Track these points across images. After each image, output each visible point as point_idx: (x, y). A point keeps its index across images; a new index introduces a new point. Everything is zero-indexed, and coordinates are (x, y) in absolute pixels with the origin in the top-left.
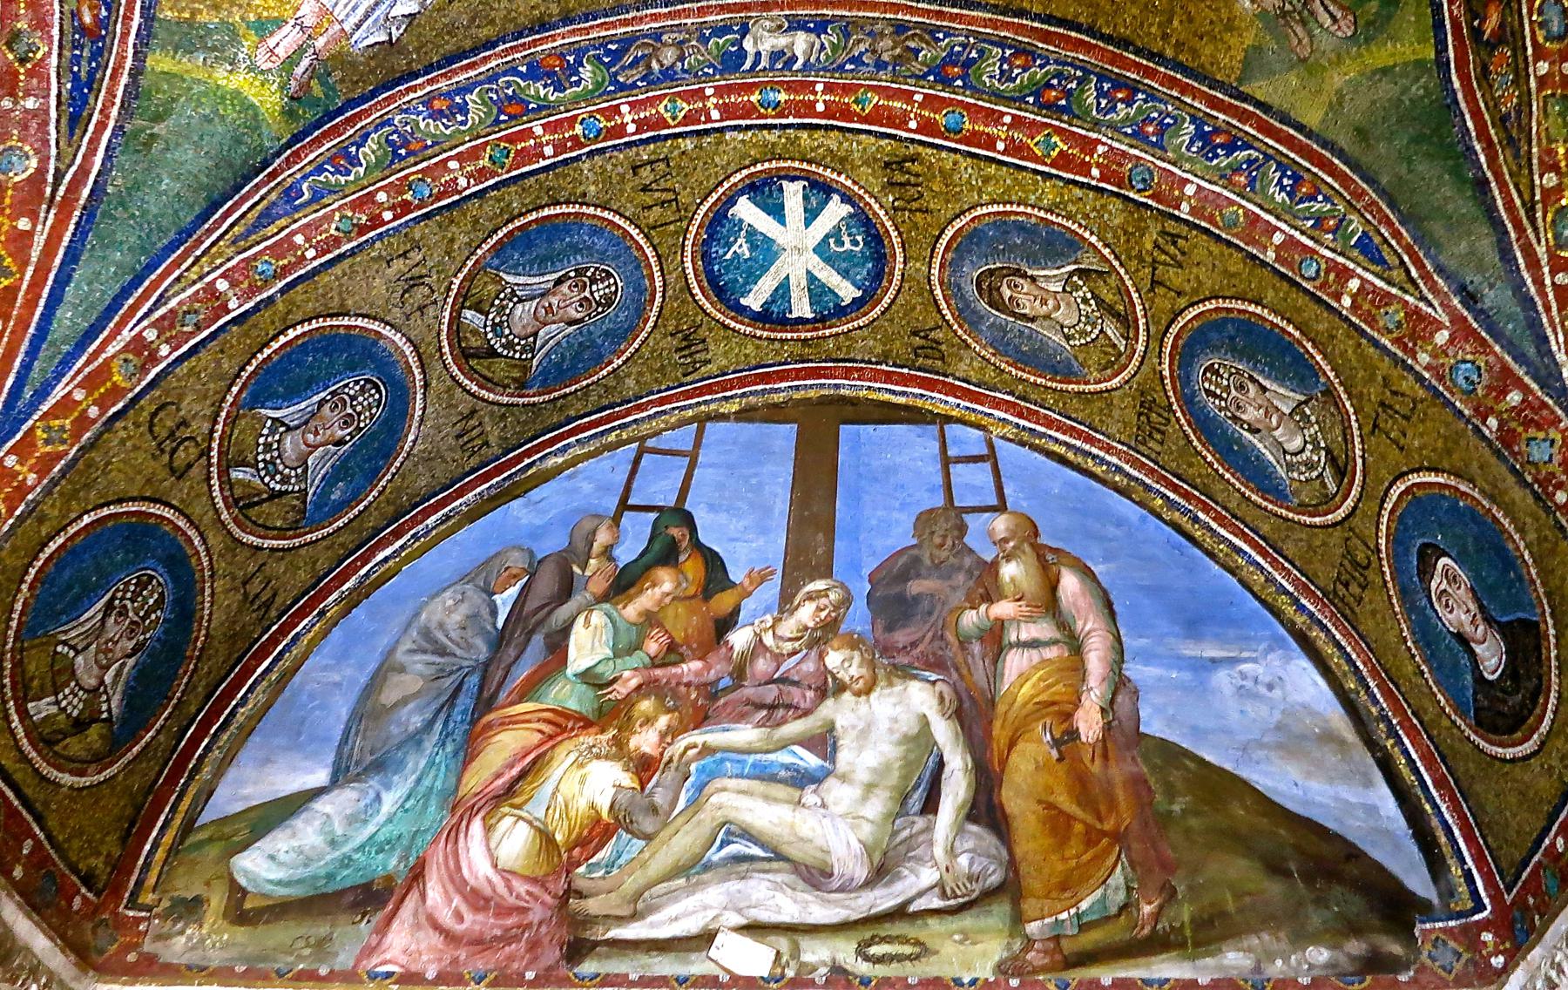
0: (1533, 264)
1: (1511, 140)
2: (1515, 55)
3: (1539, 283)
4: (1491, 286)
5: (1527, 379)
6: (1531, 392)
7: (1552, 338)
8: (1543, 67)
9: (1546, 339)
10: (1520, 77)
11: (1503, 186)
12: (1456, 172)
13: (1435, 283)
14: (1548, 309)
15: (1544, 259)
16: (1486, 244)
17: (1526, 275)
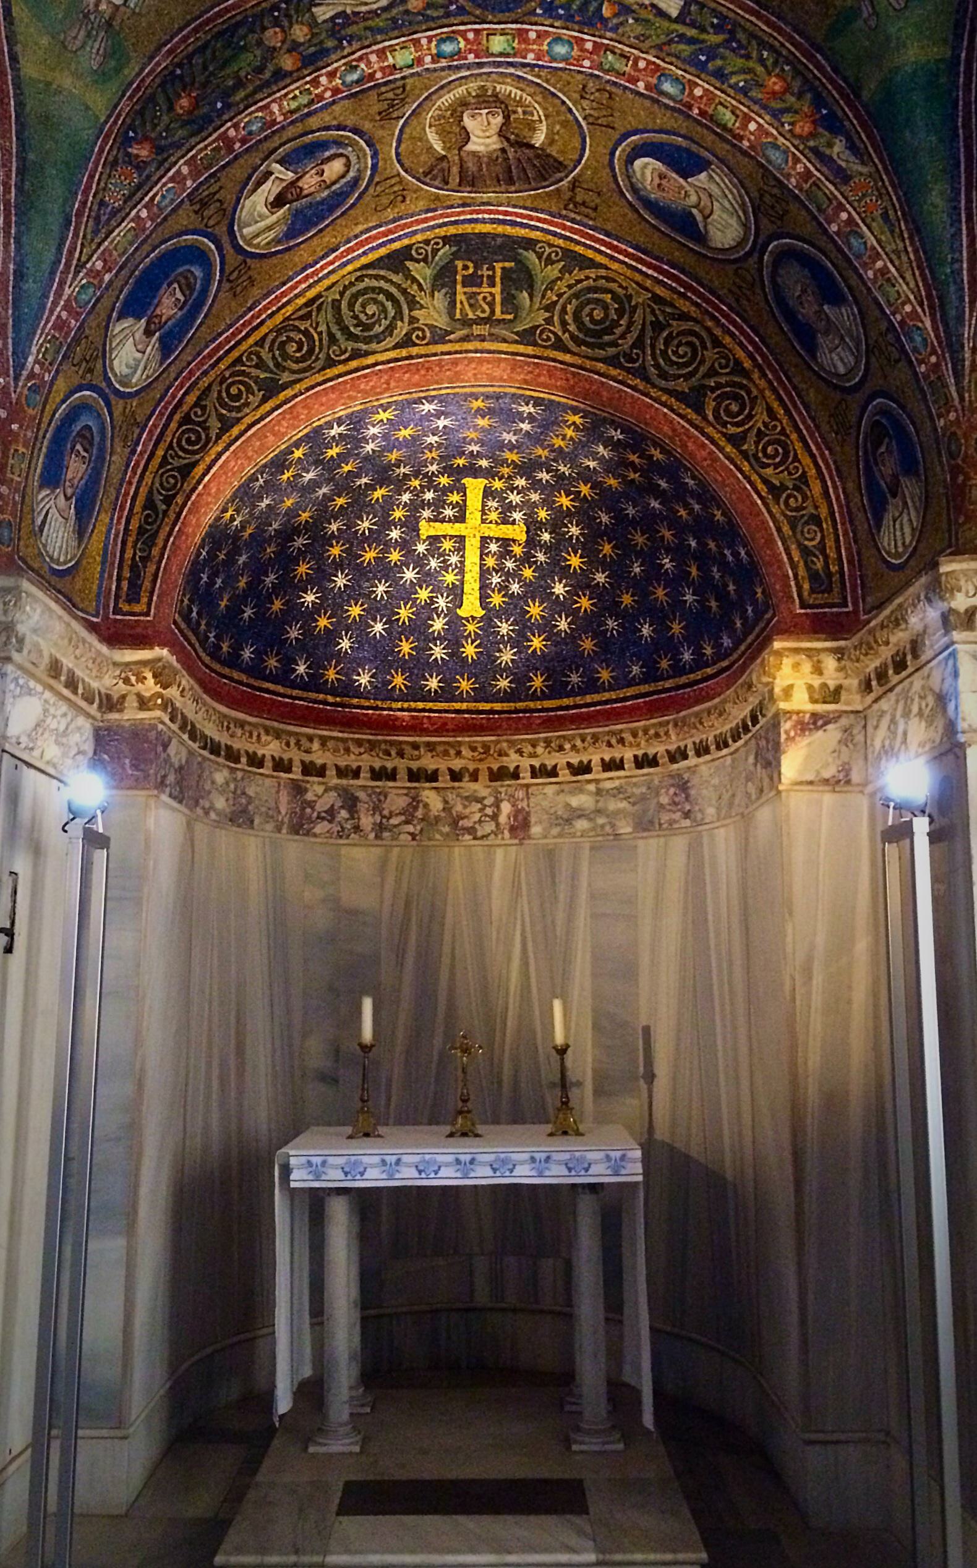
0: (59, 294)
1: (97, 219)
2: (139, 187)
3: (55, 304)
4: (34, 282)
5: (10, 341)
6: (7, 349)
7: (38, 336)
8: (144, 214)
9: (34, 334)
10: (131, 198)
11: (76, 235)
12: (66, 200)
13: (9, 244)
14: (47, 322)
15: (65, 297)
16: (49, 256)
17: (52, 295)
